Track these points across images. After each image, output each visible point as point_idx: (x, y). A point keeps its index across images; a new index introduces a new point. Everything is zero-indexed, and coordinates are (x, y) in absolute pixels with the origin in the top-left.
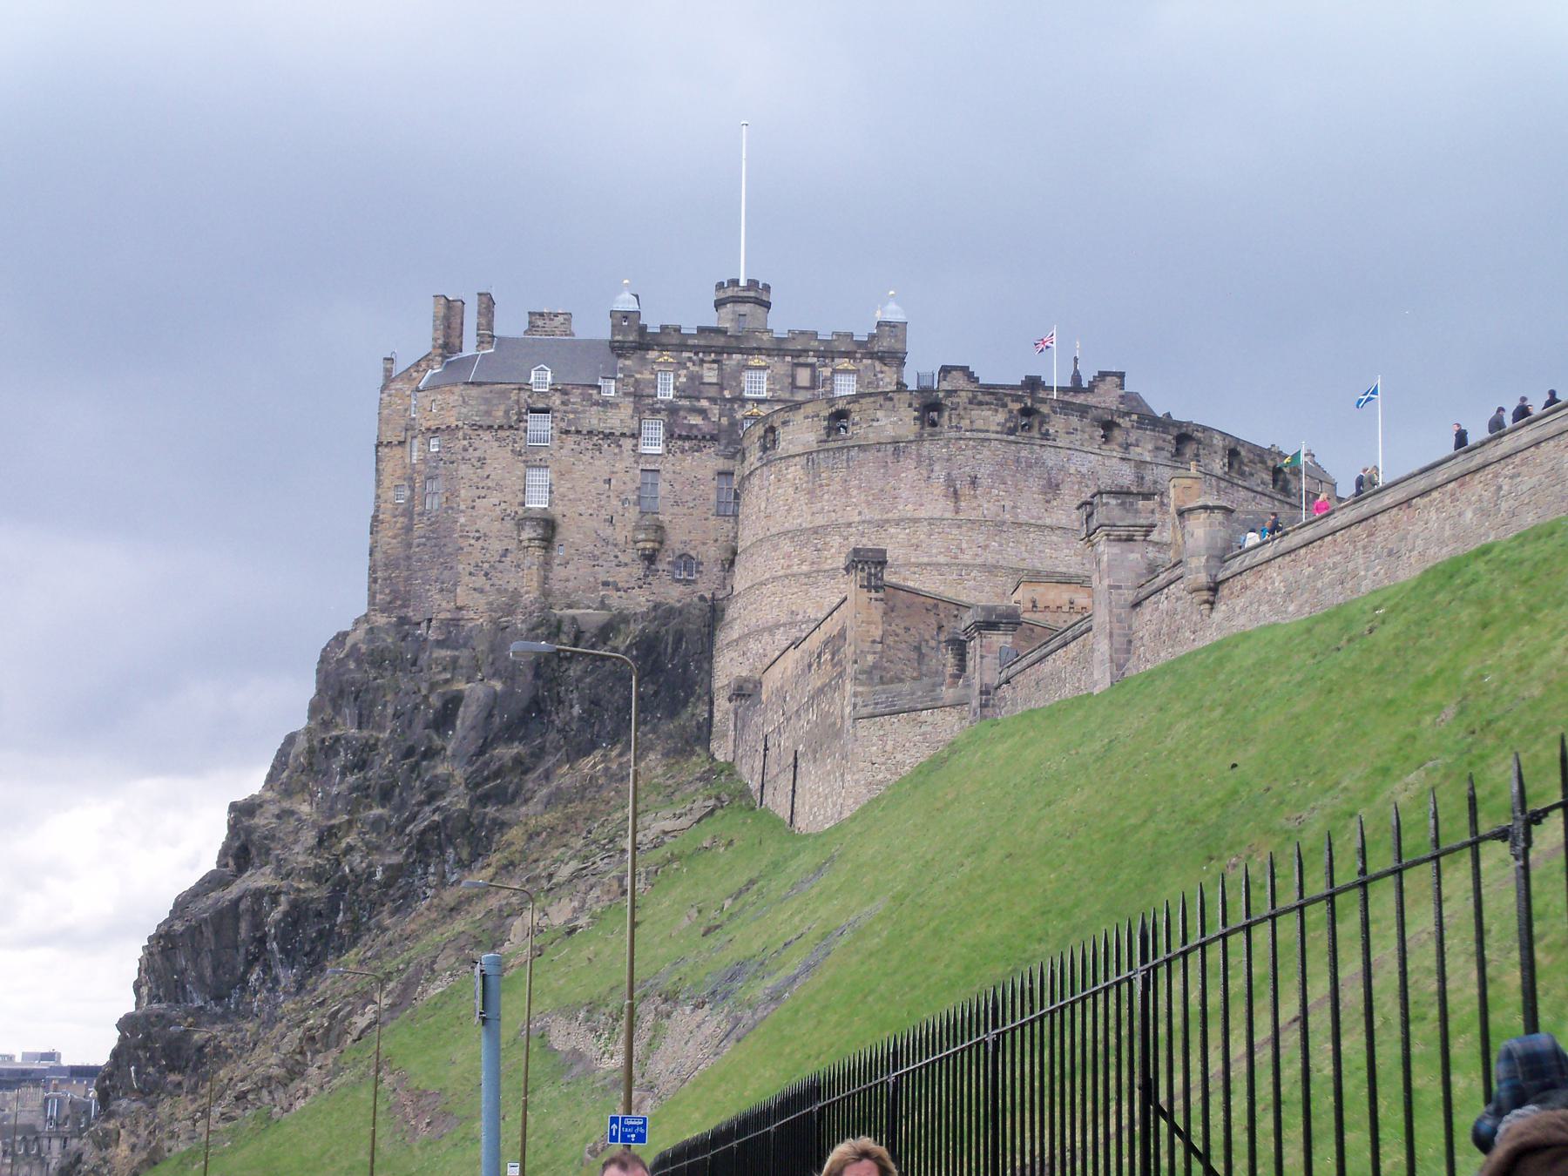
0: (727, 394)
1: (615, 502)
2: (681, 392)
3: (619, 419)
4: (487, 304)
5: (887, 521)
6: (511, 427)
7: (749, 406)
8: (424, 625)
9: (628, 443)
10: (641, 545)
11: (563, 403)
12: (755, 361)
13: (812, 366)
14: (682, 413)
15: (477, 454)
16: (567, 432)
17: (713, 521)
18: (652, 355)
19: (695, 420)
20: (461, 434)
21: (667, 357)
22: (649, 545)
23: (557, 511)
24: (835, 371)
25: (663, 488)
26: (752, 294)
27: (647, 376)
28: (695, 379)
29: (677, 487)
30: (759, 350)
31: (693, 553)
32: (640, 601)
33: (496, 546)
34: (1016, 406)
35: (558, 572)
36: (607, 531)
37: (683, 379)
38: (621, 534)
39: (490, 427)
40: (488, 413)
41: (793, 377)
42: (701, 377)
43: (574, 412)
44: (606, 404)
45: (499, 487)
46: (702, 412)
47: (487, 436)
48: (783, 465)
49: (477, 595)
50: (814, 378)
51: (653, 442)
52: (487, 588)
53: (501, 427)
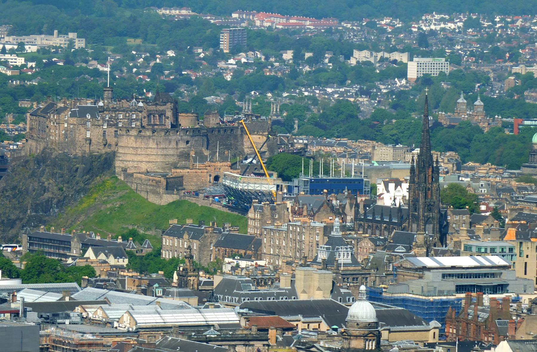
3: (101, 122)
25: (107, 133)
28: (111, 116)
32: (103, 151)
33: (82, 143)
35: (91, 147)
38: (101, 141)
44: (98, 120)
46: (113, 121)
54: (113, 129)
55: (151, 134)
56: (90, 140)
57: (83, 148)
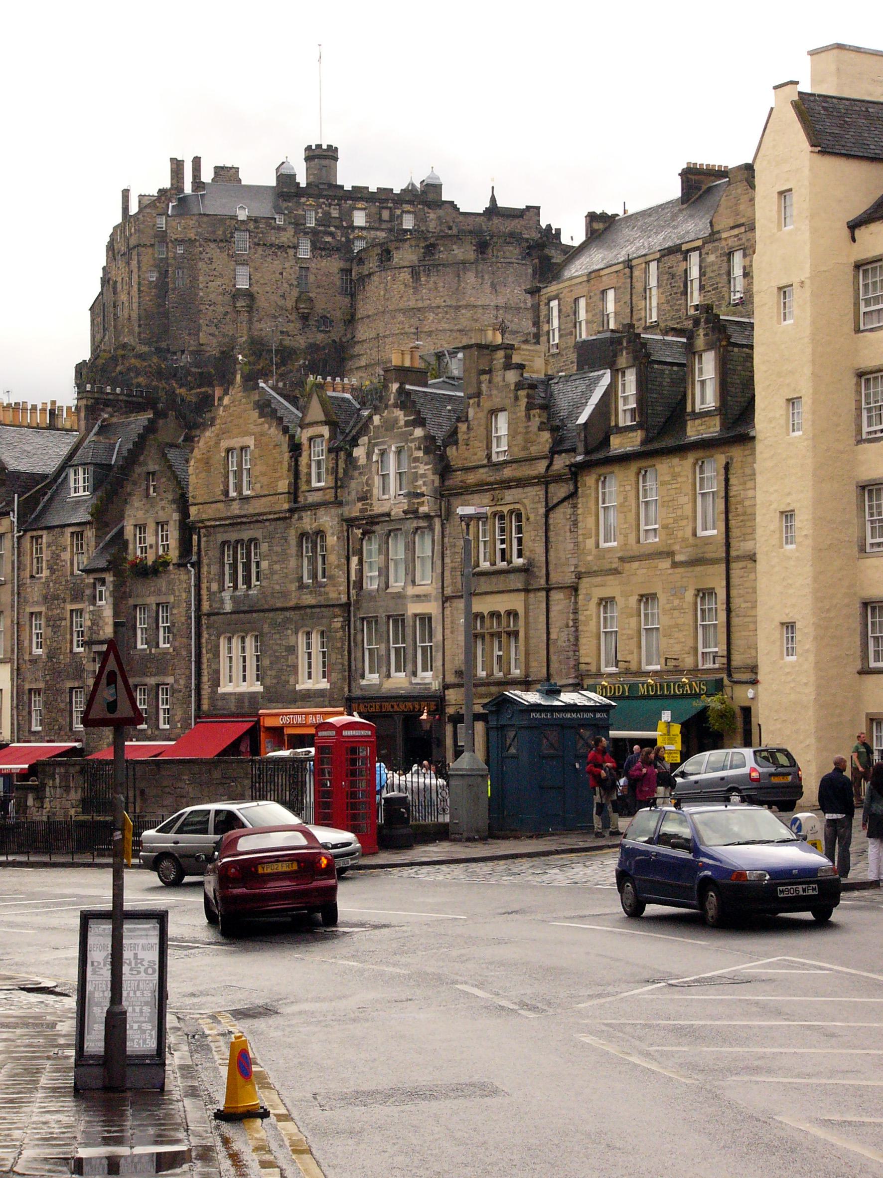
0: (344, 224)
1: (285, 285)
2: (319, 222)
3: (286, 237)
4: (197, 161)
5: (460, 306)
6: (227, 241)
7: (356, 231)
8: (179, 354)
9: (291, 252)
10: (301, 311)
11: (255, 228)
12: (360, 205)
13: (390, 208)
14: (321, 235)
15: (209, 255)
16: (259, 245)
17: (339, 298)
18: (303, 200)
19: (328, 239)
20: (197, 243)
21: (311, 201)
22: (306, 311)
23: (255, 289)
24: (403, 212)
25: (312, 278)
26: (330, 154)
27: (301, 212)
28: (327, 214)
29: (319, 277)
30: (361, 199)
31: (328, 315)
32: (301, 342)
33: (220, 309)
34: (526, 244)
36: (281, 302)
37: (320, 215)
38: (290, 303)
39: (215, 241)
40: (214, 232)
41: (380, 214)
42: (330, 213)
43: (262, 233)
44: (279, 228)
45: (221, 276)
46: (331, 234)
47: (213, 245)
48: (397, 272)
49: (211, 337)
50: (392, 215)
51: (305, 251)
52: (217, 333)
53: (221, 241)
54: (333, 265)
55: (472, 256)
56: (249, 295)
57: (229, 329)
